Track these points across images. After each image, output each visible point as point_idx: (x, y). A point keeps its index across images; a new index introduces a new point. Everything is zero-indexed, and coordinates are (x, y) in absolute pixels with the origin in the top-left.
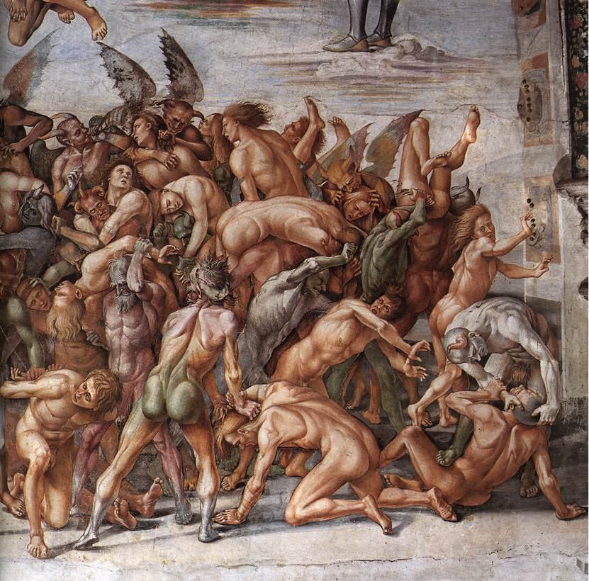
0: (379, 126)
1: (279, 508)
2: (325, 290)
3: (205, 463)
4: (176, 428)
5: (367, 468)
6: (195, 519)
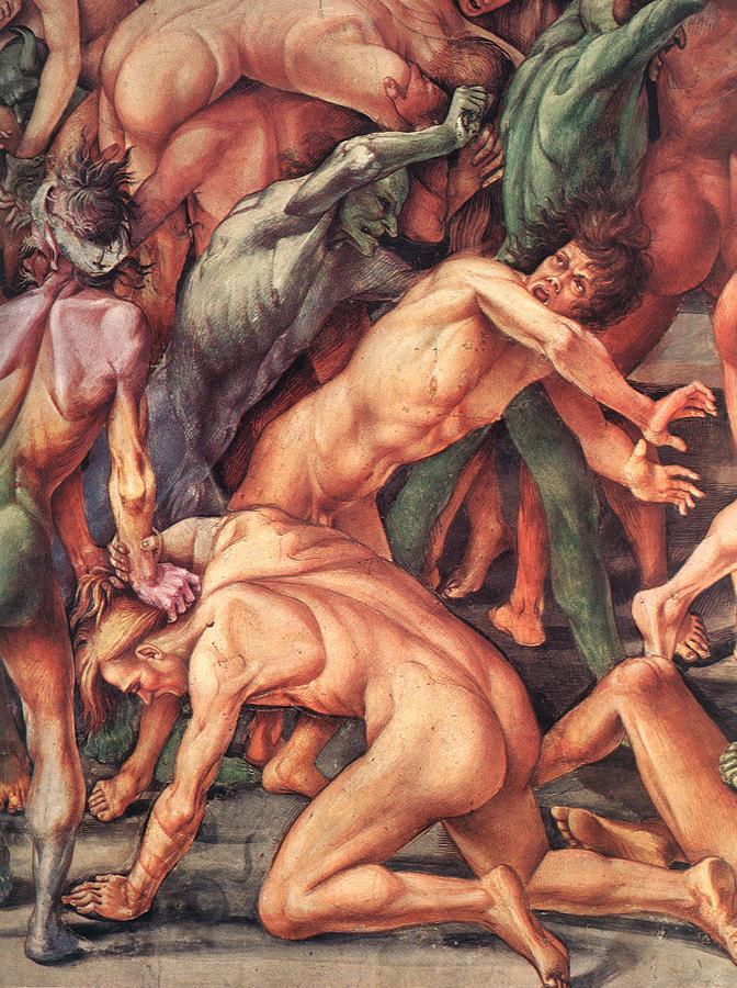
2: (393, 233)
5: (500, 784)
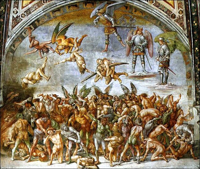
0: (165, 97)
1: (150, 158)
3: (138, 151)
4: (133, 145)
6: (136, 160)
